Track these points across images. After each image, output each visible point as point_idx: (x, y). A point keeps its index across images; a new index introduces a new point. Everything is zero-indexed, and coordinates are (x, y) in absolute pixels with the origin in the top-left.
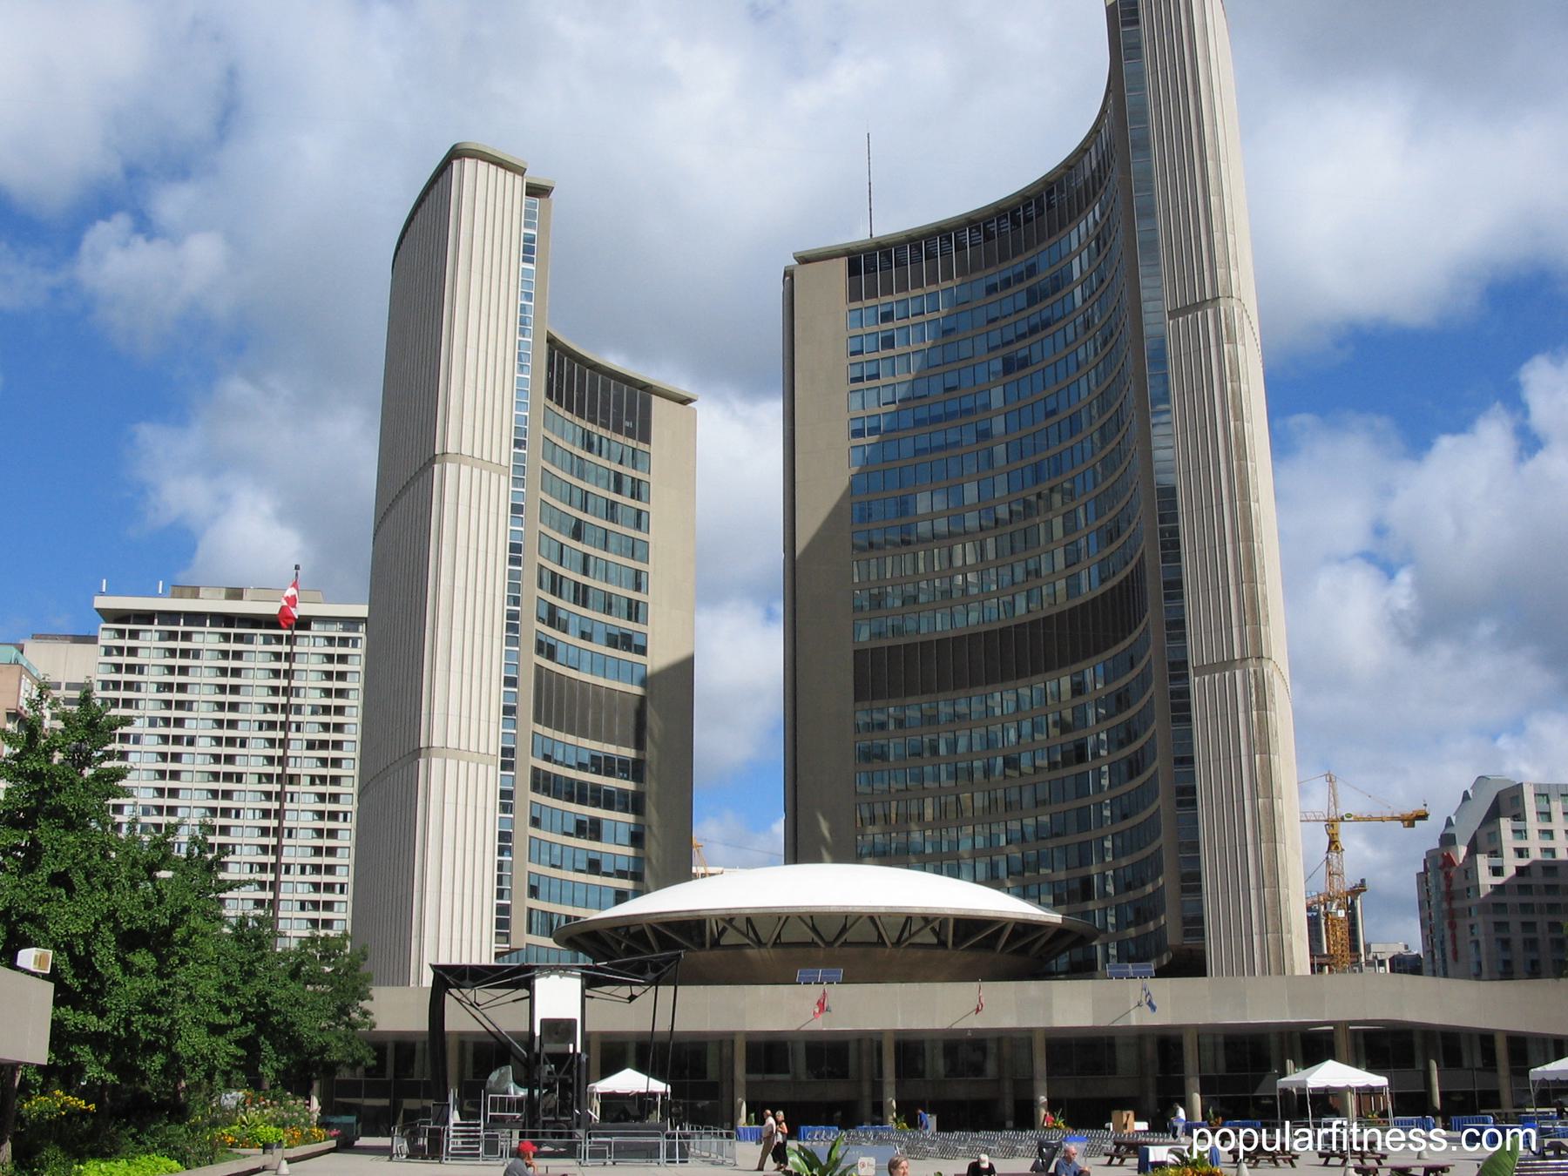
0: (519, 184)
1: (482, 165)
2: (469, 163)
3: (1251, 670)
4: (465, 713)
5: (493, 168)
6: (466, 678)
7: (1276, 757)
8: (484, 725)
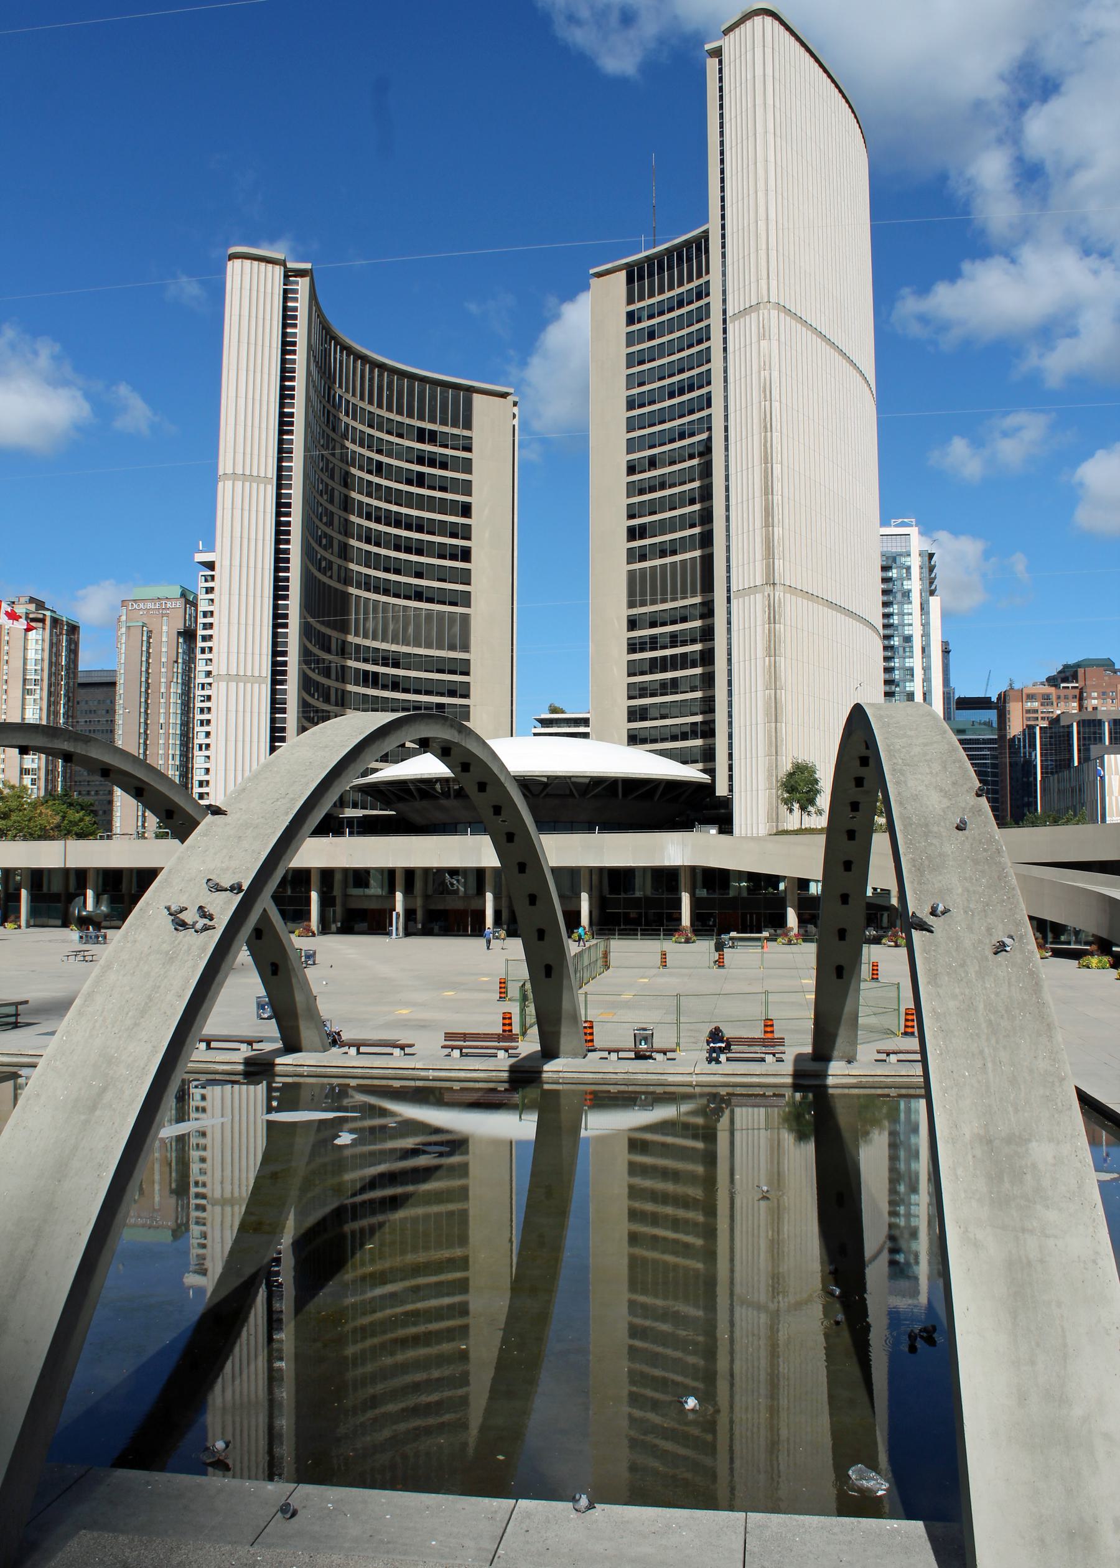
0: (279, 271)
1: (247, 262)
2: (238, 262)
3: (766, 594)
4: (242, 650)
5: (256, 263)
6: (243, 627)
7: (783, 659)
8: (257, 657)
